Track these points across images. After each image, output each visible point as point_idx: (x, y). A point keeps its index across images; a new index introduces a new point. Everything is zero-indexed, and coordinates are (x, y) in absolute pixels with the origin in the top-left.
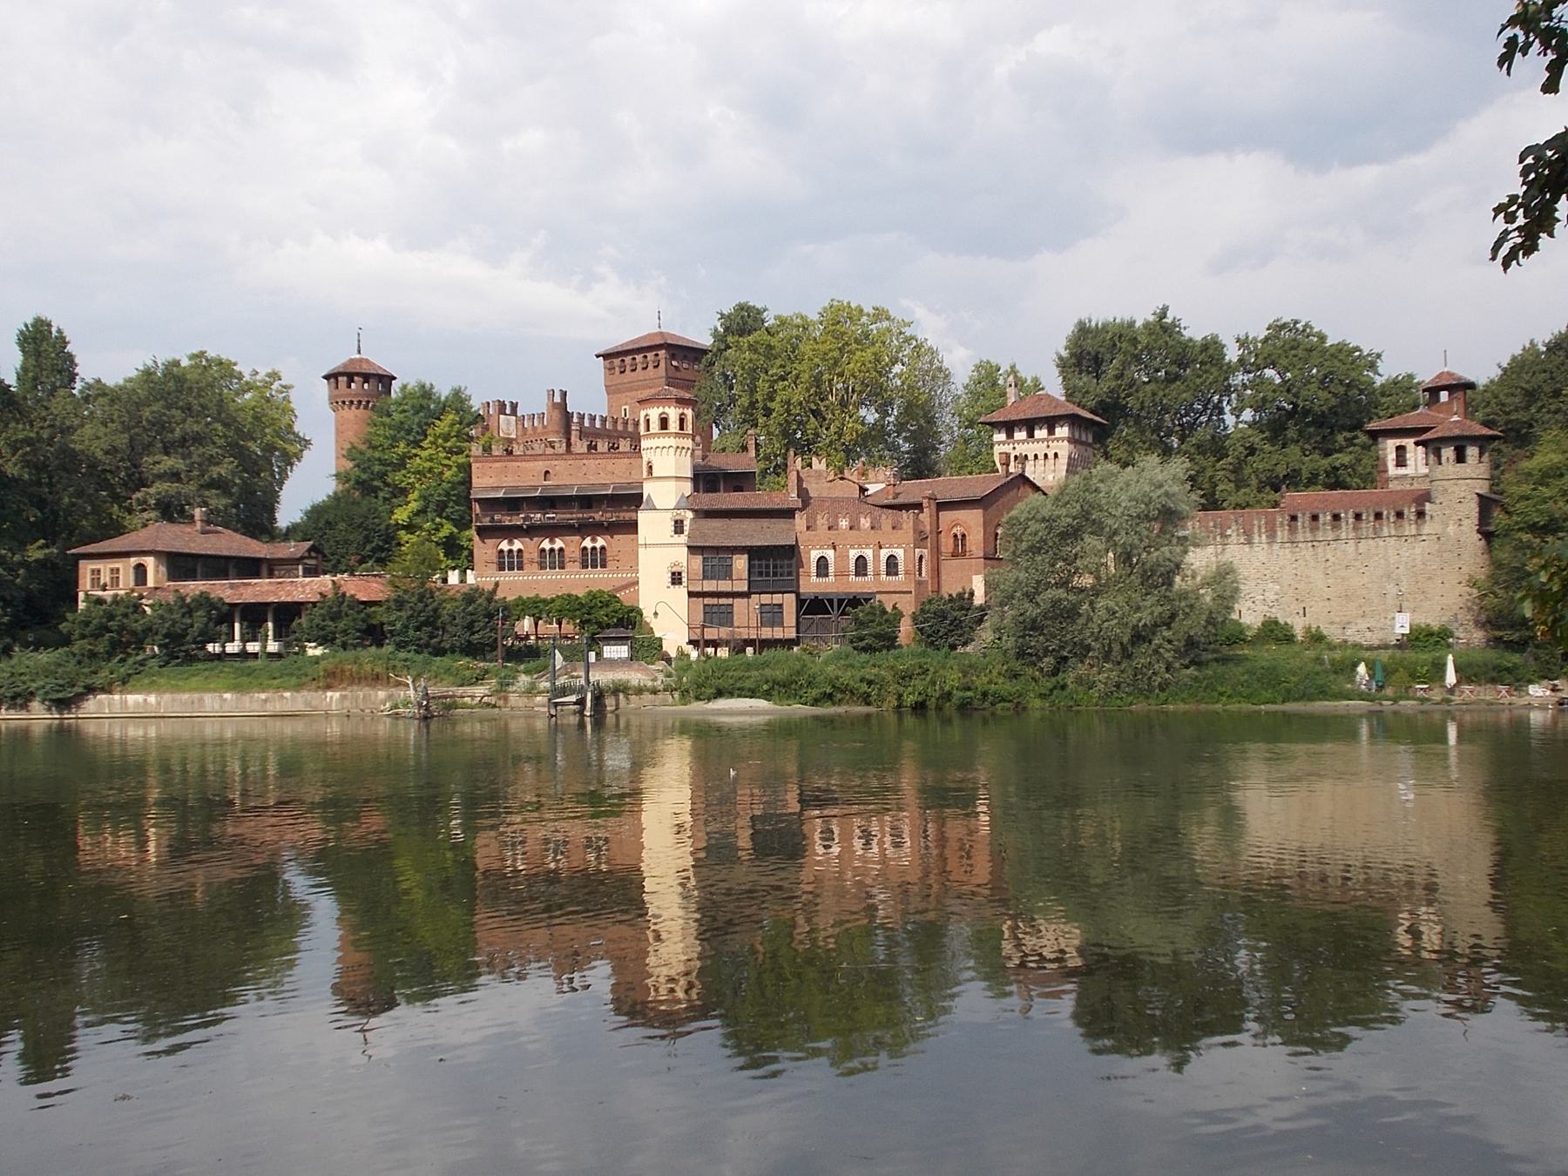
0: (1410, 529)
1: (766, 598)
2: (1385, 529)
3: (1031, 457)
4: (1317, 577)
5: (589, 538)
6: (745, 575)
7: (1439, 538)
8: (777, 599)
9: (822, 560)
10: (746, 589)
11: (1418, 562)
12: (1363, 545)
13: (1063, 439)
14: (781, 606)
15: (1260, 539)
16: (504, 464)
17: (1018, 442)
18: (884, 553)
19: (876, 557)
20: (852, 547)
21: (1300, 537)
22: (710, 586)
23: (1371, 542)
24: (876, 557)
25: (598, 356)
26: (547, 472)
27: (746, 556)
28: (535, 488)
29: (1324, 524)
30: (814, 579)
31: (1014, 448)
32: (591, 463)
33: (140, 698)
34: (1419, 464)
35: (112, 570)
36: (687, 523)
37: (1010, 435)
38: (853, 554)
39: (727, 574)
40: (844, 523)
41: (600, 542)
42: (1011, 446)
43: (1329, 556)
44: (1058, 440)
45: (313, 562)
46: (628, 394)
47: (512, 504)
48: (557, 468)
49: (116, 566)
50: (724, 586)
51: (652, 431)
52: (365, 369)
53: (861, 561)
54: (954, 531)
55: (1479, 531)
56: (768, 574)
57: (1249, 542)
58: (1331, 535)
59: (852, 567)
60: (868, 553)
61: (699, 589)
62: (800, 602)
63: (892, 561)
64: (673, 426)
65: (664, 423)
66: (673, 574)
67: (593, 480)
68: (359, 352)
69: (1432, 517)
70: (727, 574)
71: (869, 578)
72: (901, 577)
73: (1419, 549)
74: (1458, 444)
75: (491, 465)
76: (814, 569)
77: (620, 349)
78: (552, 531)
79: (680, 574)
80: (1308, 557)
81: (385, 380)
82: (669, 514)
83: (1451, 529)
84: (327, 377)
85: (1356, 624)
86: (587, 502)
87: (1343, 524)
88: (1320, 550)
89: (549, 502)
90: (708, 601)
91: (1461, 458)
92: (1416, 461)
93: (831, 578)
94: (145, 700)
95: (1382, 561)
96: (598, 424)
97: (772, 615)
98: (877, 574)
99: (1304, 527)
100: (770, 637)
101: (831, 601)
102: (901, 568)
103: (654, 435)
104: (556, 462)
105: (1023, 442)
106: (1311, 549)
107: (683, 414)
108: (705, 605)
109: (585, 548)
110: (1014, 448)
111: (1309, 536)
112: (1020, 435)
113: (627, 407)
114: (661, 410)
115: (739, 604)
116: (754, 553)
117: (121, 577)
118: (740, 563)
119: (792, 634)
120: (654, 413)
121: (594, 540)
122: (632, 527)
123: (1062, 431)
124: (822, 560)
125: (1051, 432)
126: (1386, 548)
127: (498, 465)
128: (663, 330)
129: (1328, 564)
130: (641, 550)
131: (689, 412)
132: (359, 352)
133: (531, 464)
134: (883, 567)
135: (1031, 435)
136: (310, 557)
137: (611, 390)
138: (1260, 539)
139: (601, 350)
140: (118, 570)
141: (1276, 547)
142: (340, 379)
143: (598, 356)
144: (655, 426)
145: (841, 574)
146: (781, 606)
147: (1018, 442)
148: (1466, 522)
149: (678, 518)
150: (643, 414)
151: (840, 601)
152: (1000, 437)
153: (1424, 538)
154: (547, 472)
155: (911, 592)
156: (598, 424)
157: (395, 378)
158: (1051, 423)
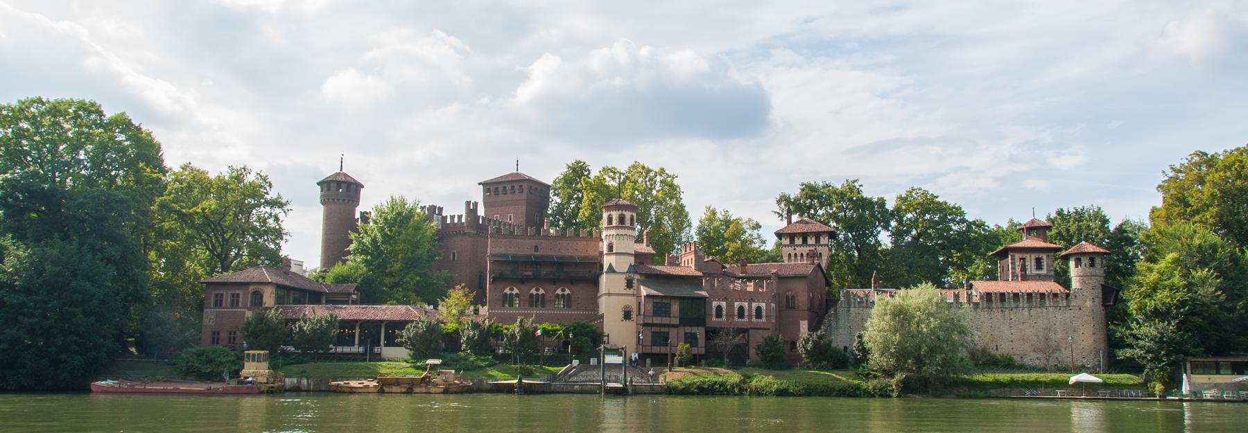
1: (688, 330)
2: (1047, 303)
4: (1005, 328)
5: (560, 289)
7: (1080, 309)
8: (694, 330)
9: (719, 308)
10: (678, 323)
11: (1068, 321)
12: (1033, 312)
13: (825, 245)
17: (797, 246)
18: (754, 305)
19: (750, 307)
21: (994, 305)
22: (657, 320)
23: (1038, 309)
24: (750, 307)
25: (479, 184)
26: (536, 247)
27: (678, 303)
28: (529, 257)
29: (1009, 299)
30: (714, 319)
31: (795, 249)
32: (564, 243)
33: (295, 380)
34: (1033, 268)
35: (233, 295)
37: (792, 241)
38: (737, 304)
39: (667, 313)
42: (793, 248)
43: (1012, 317)
44: (822, 245)
45: (354, 297)
46: (500, 208)
49: (237, 292)
50: (665, 320)
51: (614, 224)
53: (741, 309)
54: (787, 294)
55: (1103, 305)
58: (1013, 305)
59: (736, 313)
60: (746, 305)
61: (651, 322)
62: (707, 332)
63: (759, 309)
64: (628, 223)
65: (622, 219)
66: (625, 312)
67: (565, 253)
68: (341, 170)
69: (1076, 296)
70: (667, 313)
71: (746, 319)
72: (764, 319)
73: (1068, 314)
74: (1091, 256)
75: (501, 240)
76: (714, 313)
77: (496, 181)
78: (536, 280)
80: (998, 317)
83: (1088, 304)
84: (319, 184)
85: (1030, 356)
87: (1021, 299)
90: (655, 329)
91: (1092, 265)
92: (1031, 266)
93: (724, 318)
94: (299, 382)
95: (1045, 320)
98: (750, 316)
99: (996, 300)
102: (764, 313)
103: (616, 227)
104: (543, 241)
105: (800, 246)
106: (1000, 312)
107: (632, 216)
108: (653, 332)
110: (795, 249)
111: (999, 305)
113: (498, 216)
114: (620, 212)
116: (681, 299)
117: (241, 299)
118: (675, 308)
119: (702, 351)
122: (595, 283)
123: (824, 240)
124: (719, 308)
125: (818, 240)
126: (1048, 313)
127: (505, 240)
128: (519, 171)
129: (1011, 321)
131: (635, 215)
132: (341, 170)
134: (754, 313)
136: (354, 294)
139: (482, 181)
140: (238, 295)
141: (979, 311)
142: (332, 184)
143: (479, 184)
145: (730, 315)
147: (797, 246)
148: (1096, 300)
149: (629, 278)
150: (605, 215)
153: (1071, 308)
155: (769, 329)
157: (363, 187)
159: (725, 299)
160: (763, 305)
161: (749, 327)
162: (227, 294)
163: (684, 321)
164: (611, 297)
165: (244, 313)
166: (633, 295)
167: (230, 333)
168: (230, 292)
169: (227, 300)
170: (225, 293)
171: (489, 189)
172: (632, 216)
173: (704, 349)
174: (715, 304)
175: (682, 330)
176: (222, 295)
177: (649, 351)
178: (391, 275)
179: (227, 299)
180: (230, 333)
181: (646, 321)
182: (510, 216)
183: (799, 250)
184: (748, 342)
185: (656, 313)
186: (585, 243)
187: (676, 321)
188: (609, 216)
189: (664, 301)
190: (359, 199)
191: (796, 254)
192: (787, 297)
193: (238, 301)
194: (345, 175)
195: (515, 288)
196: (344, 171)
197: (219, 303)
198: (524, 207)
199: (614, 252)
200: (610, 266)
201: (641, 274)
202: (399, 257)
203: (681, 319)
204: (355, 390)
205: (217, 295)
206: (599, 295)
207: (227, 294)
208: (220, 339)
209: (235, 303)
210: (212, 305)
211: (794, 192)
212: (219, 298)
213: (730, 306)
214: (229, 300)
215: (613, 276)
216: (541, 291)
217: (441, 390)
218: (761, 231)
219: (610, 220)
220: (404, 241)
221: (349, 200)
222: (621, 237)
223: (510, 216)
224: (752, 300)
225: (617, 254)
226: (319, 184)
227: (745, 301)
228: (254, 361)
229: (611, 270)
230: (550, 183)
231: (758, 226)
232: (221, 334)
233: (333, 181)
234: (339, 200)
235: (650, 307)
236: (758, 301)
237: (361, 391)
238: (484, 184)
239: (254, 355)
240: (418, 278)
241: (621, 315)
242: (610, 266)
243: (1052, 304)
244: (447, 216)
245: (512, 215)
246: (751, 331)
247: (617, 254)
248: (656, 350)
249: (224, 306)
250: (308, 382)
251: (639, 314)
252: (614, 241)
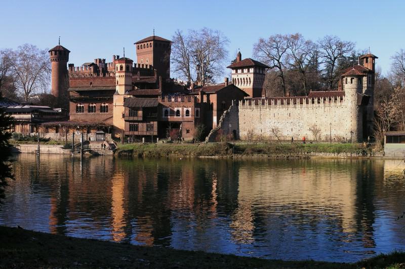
0: (338, 103)
3: (242, 79)
8: (152, 123)
15: (298, 105)
18: (185, 109)
19: (183, 109)
22: (131, 118)
24: (183, 109)
30: (164, 117)
40: (173, 100)
41: (94, 105)
44: (250, 73)
50: (135, 118)
57: (295, 107)
58: (317, 105)
60: (180, 109)
63: (188, 112)
65: (121, 68)
70: (136, 115)
72: (190, 117)
88: (315, 110)
102: (190, 113)
105: (240, 74)
115: (140, 125)
118: (140, 113)
123: (252, 70)
130: (114, 107)
135: (237, 72)
137: (138, 54)
138: (298, 105)
139: (136, 42)
157: (70, 52)
158: (248, 67)
160: (190, 109)
161: (181, 121)
187: (141, 119)
191: (238, 79)
243: (334, 105)
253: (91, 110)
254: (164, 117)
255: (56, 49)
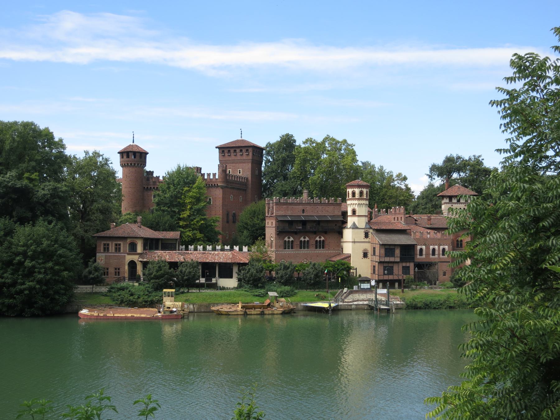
1: (404, 264)
6: (399, 255)
8: (408, 264)
10: (399, 260)
14: (409, 267)
16: (287, 206)
18: (441, 247)
19: (439, 248)
20: (431, 245)
22: (387, 259)
24: (439, 248)
25: (216, 148)
30: (418, 257)
36: (370, 234)
38: (431, 247)
47: (291, 223)
48: (307, 208)
49: (119, 243)
50: (392, 259)
52: (135, 149)
53: (434, 250)
54: (458, 239)
56: (406, 255)
59: (431, 253)
60: (436, 247)
61: (383, 260)
62: (415, 265)
66: (364, 253)
67: (320, 214)
68: (133, 142)
71: (436, 256)
75: (281, 206)
76: (418, 253)
77: (228, 146)
78: (305, 232)
79: (367, 253)
81: (143, 155)
82: (363, 230)
86: (318, 222)
89: (304, 223)
90: (386, 265)
93: (424, 256)
96: (211, 177)
97: (406, 270)
98: (439, 254)
100: (397, 278)
101: (423, 265)
103: (358, 199)
105: (456, 203)
109: (317, 241)
112: (454, 200)
113: (231, 170)
114: (360, 189)
118: (398, 252)
120: (357, 191)
121: (320, 238)
122: (341, 234)
124: (421, 250)
127: (285, 206)
128: (243, 138)
131: (368, 190)
132: (133, 142)
133: (298, 207)
134: (441, 253)
140: (120, 245)
143: (216, 148)
144: (357, 196)
145: (428, 254)
146: (409, 267)
147: (454, 203)
151: (427, 265)
152: (446, 200)
154: (303, 210)
156: (211, 177)
157: (147, 153)
159: (424, 245)
160: (446, 247)
162: (112, 244)
163: (403, 260)
164: (357, 244)
165: (125, 256)
166: (369, 242)
167: (116, 269)
168: (114, 243)
169: (112, 248)
170: (110, 243)
171: (223, 151)
172: (367, 191)
173: (413, 276)
174: (419, 247)
175: (401, 265)
176: (108, 245)
177: (382, 279)
178: (183, 219)
179: (112, 247)
180: (116, 269)
181: (381, 260)
182: (240, 171)
183: (455, 206)
184: (437, 270)
185: (387, 255)
186: (333, 207)
187: (398, 260)
188: (353, 191)
189: (391, 247)
190: (145, 162)
192: (457, 241)
193: (120, 248)
194: (137, 146)
195: (291, 237)
196: (135, 143)
197: (106, 249)
198: (250, 165)
199: (357, 215)
200: (354, 224)
201: (374, 230)
202: (188, 207)
203: (401, 258)
204: (229, 313)
205: (105, 245)
206: (342, 240)
207: (112, 244)
208: (109, 272)
209: (118, 249)
210: (102, 251)
211: (440, 162)
212: (106, 247)
213: (428, 248)
214: (114, 248)
215: (356, 230)
216: (307, 239)
217: (281, 312)
218: (407, 182)
219: (354, 194)
220: (191, 197)
221: (141, 164)
222: (361, 205)
223: (240, 171)
224: (439, 246)
225: (359, 216)
226: (118, 153)
227: (436, 245)
228: (169, 296)
229: (355, 227)
230: (262, 145)
231: (405, 179)
232: (109, 270)
233: (131, 152)
234: (135, 164)
235: (383, 251)
236: (444, 245)
237: (233, 313)
238: (220, 148)
239: (169, 292)
240: (202, 222)
241: (362, 255)
242: (354, 224)
244: (204, 174)
245: (241, 170)
246: (439, 264)
247: (359, 216)
248: (386, 277)
249: (110, 251)
250: (193, 307)
251: (374, 254)
252: (356, 208)
253: (303, 245)
254: (418, 257)
255: (128, 150)
